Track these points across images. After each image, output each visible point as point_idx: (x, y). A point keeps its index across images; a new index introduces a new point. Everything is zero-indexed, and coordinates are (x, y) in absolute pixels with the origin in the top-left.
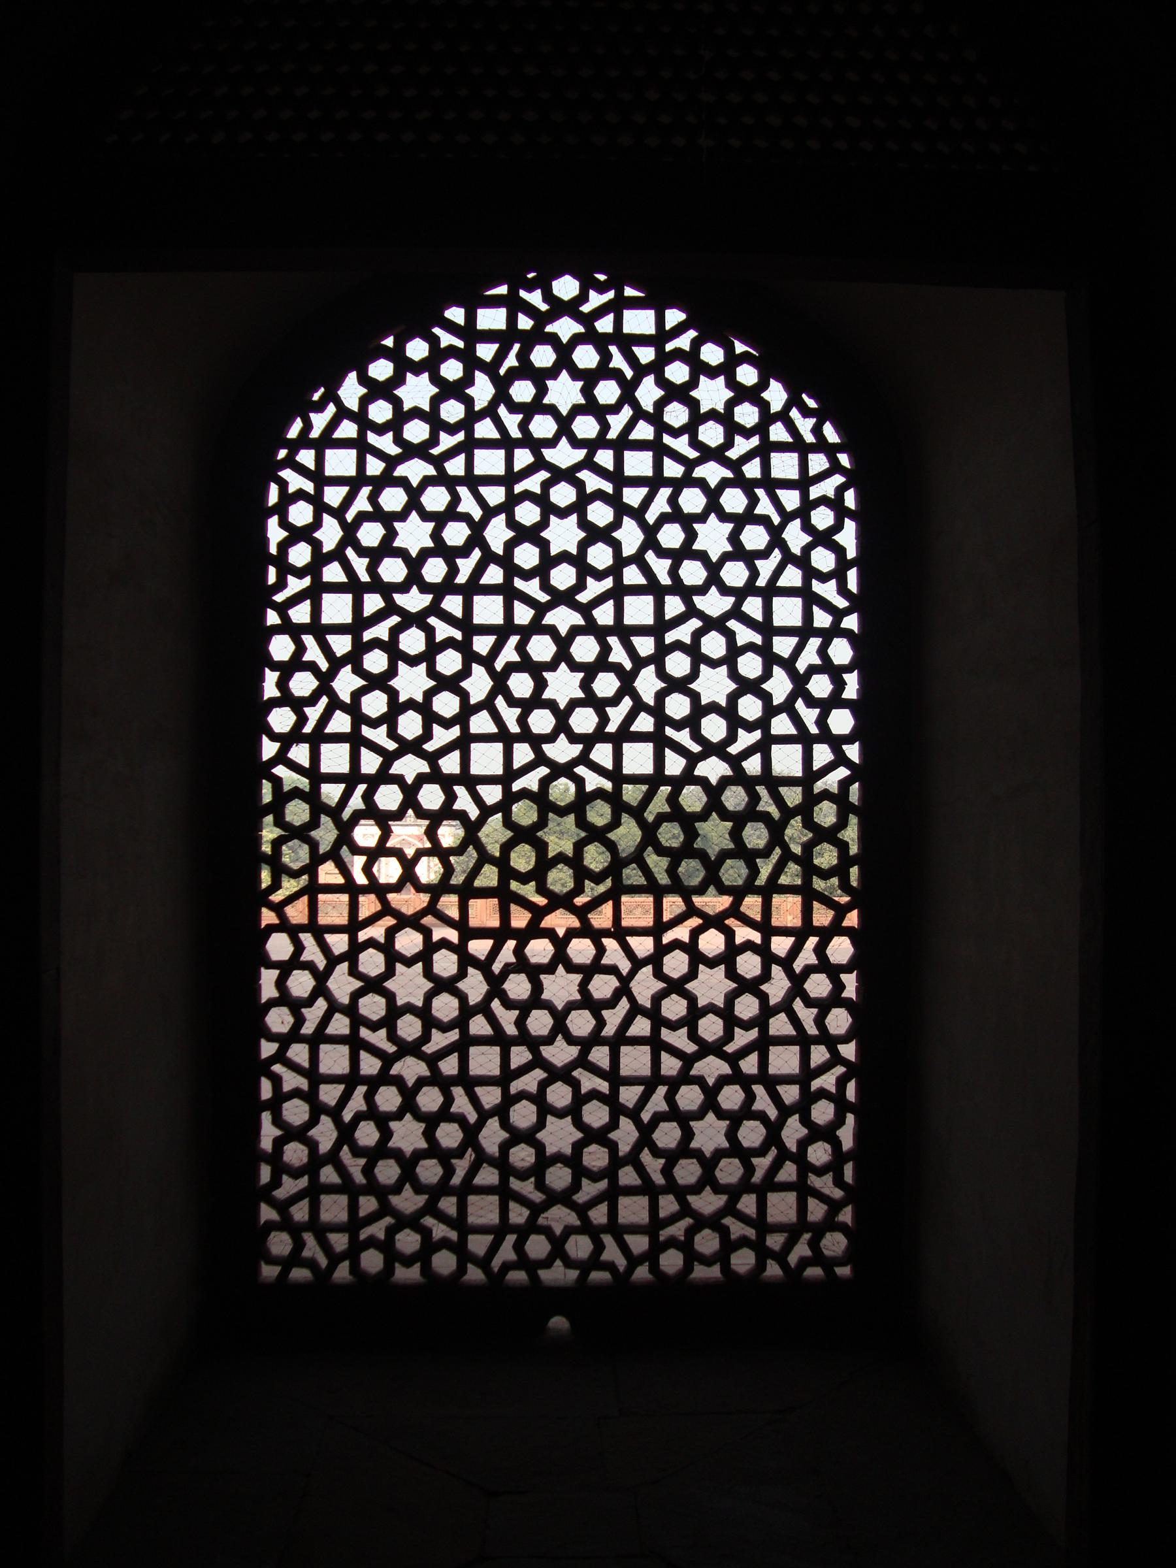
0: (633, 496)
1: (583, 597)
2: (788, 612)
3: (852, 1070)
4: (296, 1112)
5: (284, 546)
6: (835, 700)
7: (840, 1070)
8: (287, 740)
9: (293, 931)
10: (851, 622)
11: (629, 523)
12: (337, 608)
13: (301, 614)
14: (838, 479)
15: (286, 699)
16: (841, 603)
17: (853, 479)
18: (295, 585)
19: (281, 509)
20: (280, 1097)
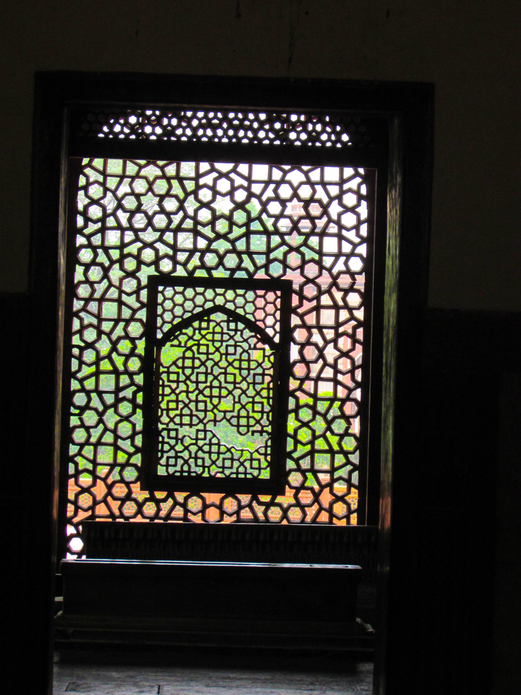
0: (256, 189)
1: (231, 236)
2: (330, 245)
3: (355, 468)
4: (86, 479)
5: (86, 207)
6: (351, 289)
7: (349, 467)
8: (87, 301)
9: (88, 393)
10: (362, 250)
11: (254, 200)
12: (113, 238)
13: (97, 240)
14: (358, 180)
15: (87, 281)
16: (357, 240)
17: (366, 179)
18: (92, 227)
19: (85, 188)
20: (78, 473)
